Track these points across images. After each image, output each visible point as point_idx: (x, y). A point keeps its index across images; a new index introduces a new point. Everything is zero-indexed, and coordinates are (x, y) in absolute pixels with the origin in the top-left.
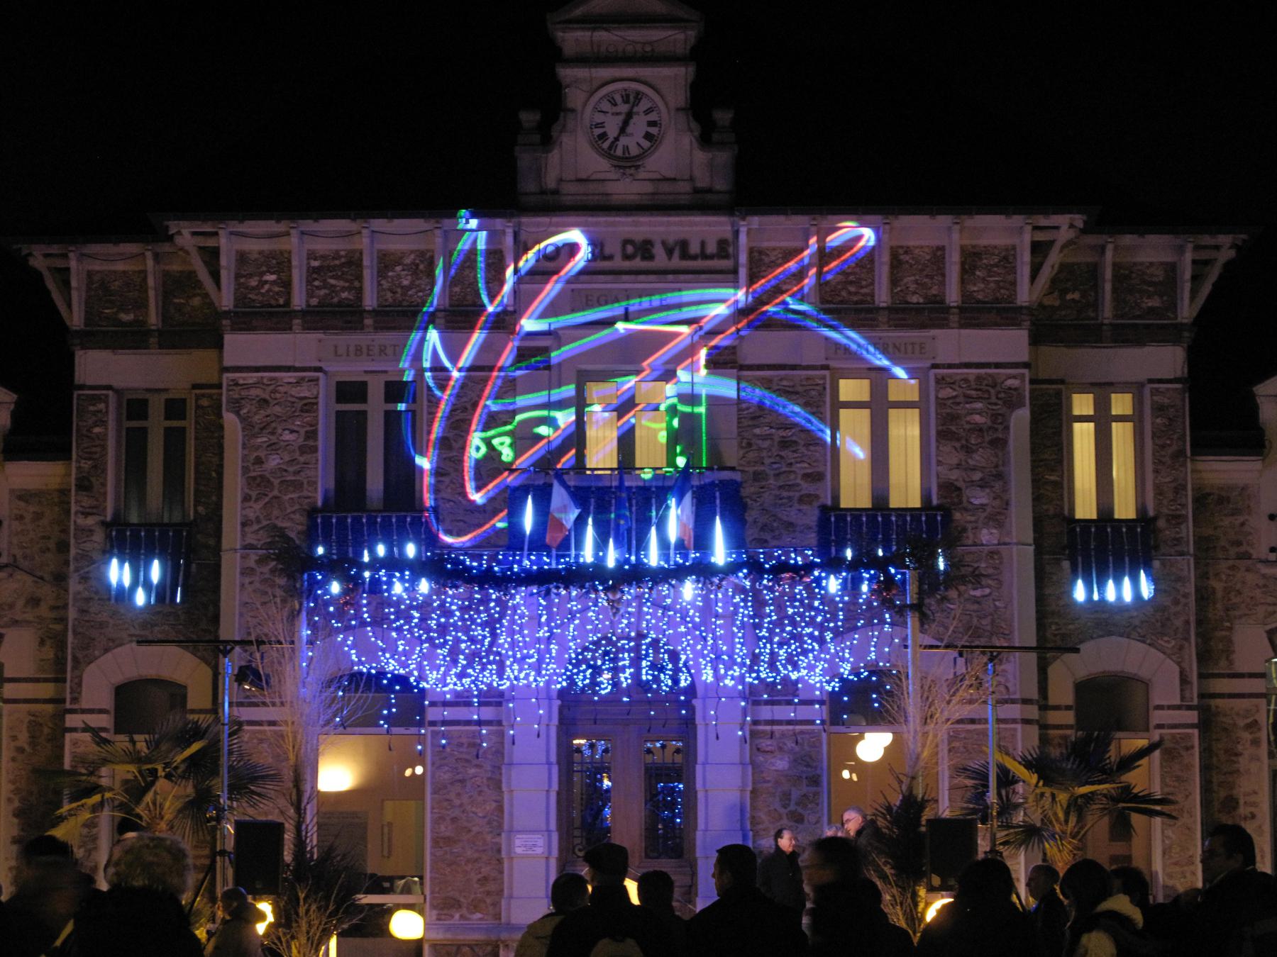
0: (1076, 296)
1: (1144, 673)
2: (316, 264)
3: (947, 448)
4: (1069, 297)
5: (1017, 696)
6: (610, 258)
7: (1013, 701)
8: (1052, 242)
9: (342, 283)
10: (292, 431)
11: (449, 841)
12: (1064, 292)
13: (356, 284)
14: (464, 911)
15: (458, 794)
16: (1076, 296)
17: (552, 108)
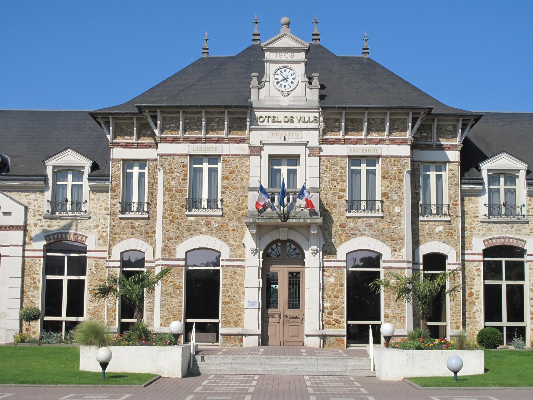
0: (425, 134)
1: (445, 253)
2: (187, 121)
3: (384, 181)
4: (423, 135)
5: (406, 260)
6: (280, 122)
7: (404, 262)
8: (418, 118)
9: (196, 127)
10: (179, 173)
11: (228, 303)
12: (421, 133)
13: (200, 128)
14: (232, 325)
15: (230, 288)
16: (425, 134)
17: (262, 73)
